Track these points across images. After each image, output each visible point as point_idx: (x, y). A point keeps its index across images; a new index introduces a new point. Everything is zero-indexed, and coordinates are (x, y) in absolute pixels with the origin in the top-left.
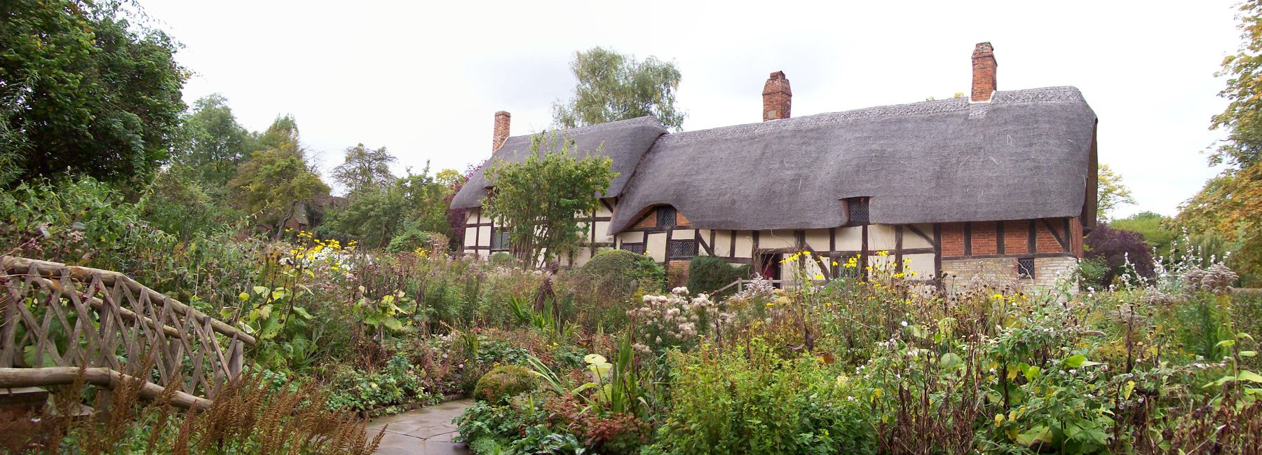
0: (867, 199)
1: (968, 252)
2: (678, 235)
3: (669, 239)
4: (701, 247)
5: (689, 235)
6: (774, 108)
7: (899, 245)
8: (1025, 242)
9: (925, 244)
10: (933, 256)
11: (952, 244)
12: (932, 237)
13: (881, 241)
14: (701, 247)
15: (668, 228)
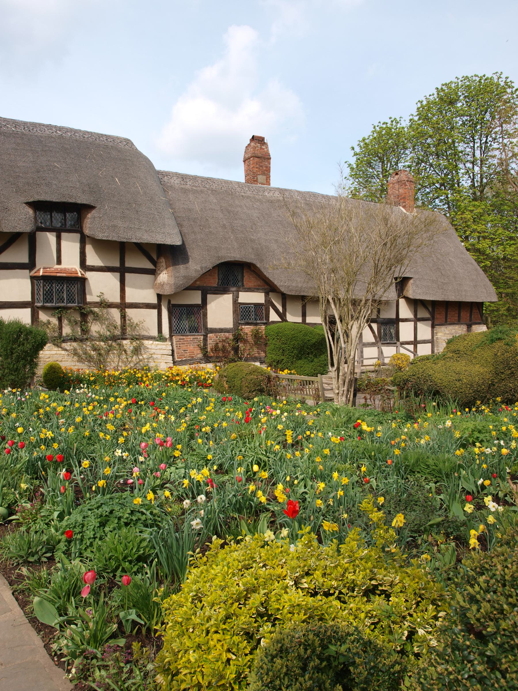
0: (411, 278)
1: (446, 321)
2: (245, 297)
3: (235, 302)
4: (272, 312)
5: (258, 298)
6: (263, 174)
7: (415, 315)
8: (468, 315)
9: (427, 315)
10: (430, 323)
11: (440, 316)
12: (430, 309)
13: (405, 311)
14: (272, 312)
15: (234, 289)
